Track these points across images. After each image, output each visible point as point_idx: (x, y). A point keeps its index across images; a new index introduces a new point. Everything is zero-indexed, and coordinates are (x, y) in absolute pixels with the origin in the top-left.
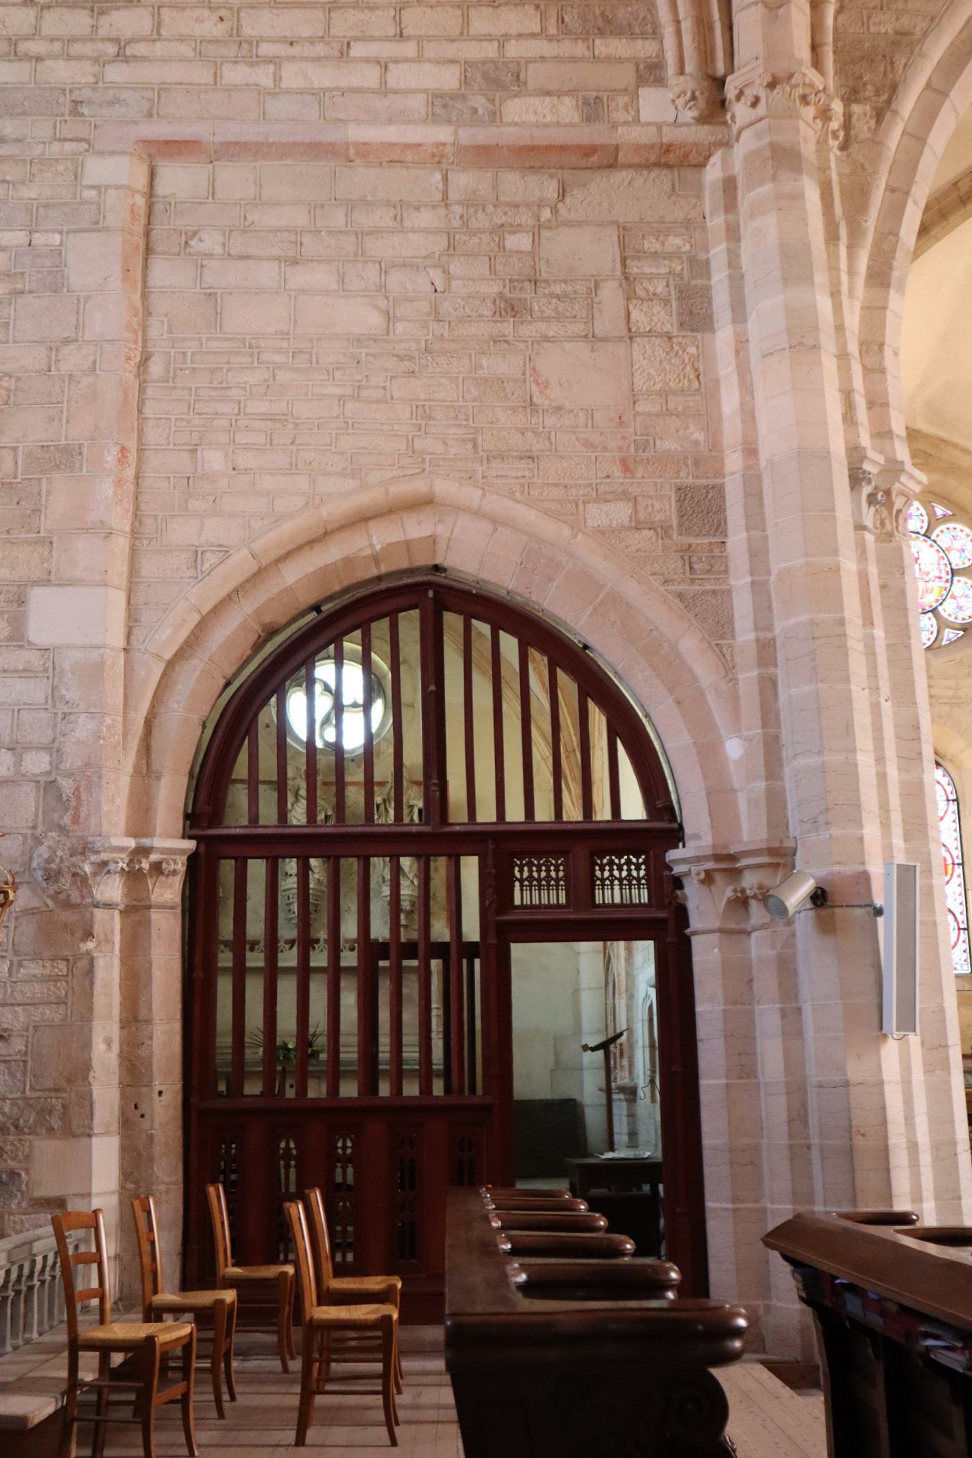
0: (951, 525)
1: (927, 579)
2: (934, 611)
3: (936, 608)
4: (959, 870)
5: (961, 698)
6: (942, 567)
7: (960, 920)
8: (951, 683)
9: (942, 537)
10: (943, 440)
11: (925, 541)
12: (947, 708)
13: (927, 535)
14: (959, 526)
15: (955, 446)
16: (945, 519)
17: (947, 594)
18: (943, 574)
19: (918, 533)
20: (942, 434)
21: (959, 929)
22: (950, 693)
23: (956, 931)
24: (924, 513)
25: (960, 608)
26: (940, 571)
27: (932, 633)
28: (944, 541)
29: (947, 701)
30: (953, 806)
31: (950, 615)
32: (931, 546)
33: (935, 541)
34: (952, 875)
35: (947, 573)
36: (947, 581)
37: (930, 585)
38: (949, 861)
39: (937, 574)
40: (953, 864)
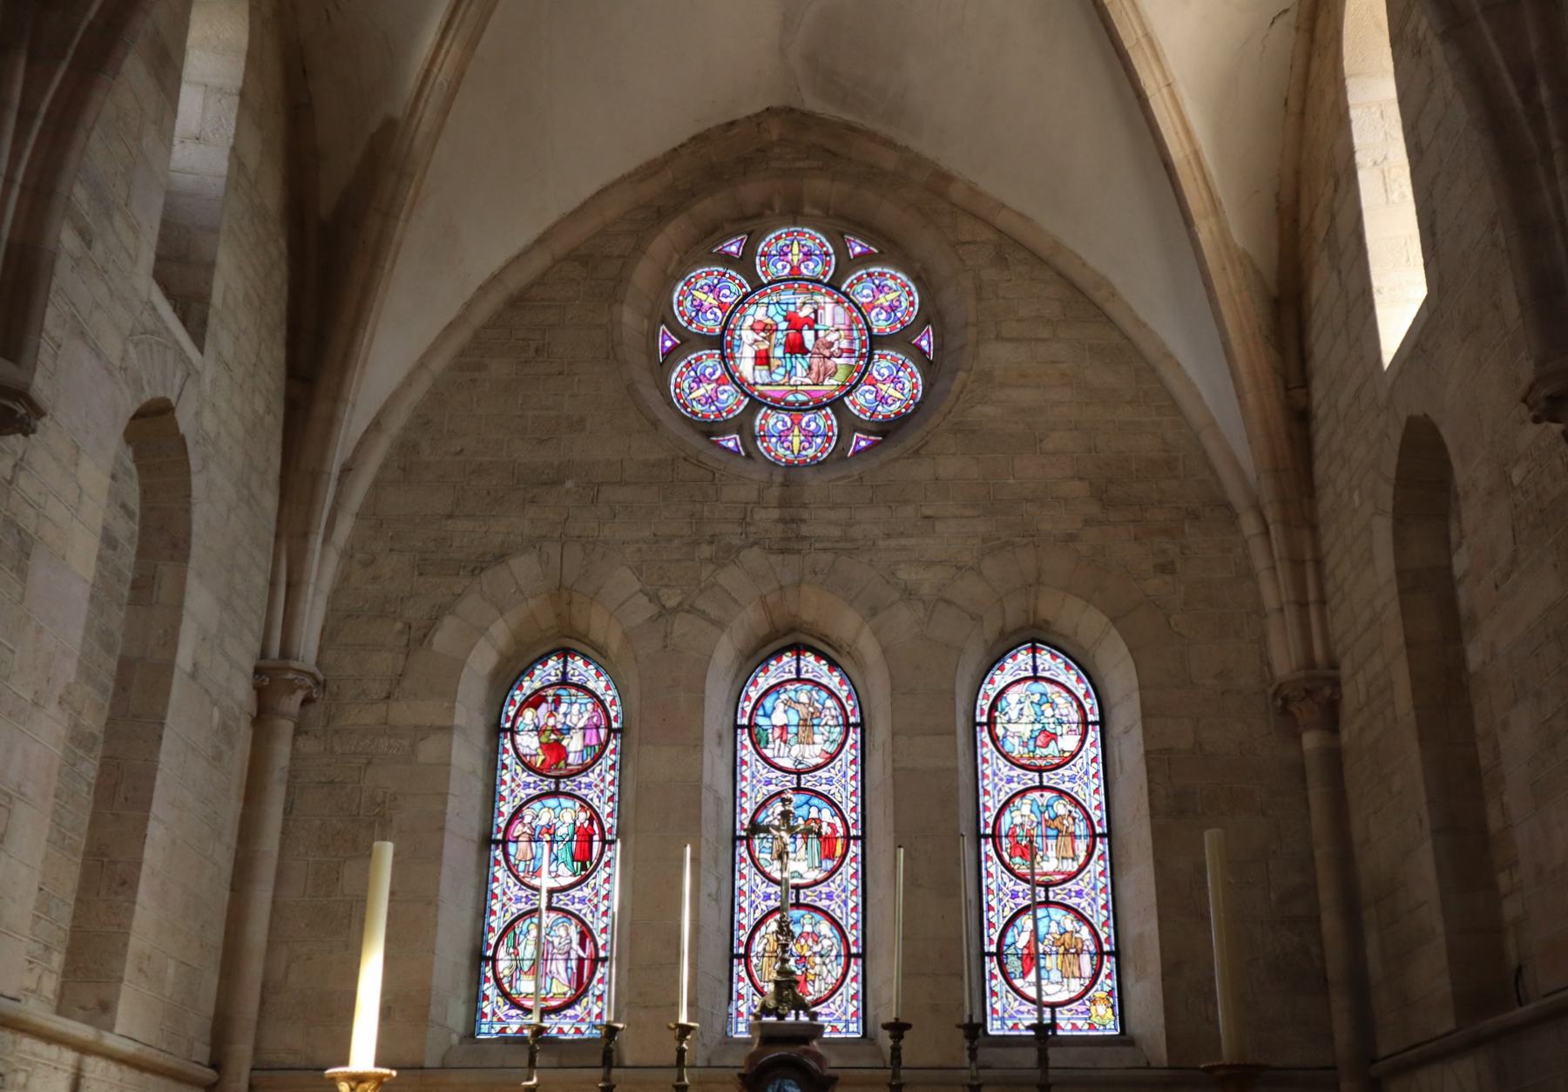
0: (875, 270)
1: (827, 353)
2: (837, 405)
3: (841, 398)
4: (855, 849)
5: (854, 540)
6: (855, 334)
7: (851, 939)
8: (842, 514)
9: (858, 288)
10: (851, 128)
11: (831, 295)
12: (827, 558)
13: (834, 285)
14: (889, 271)
15: (872, 136)
16: (865, 259)
17: (861, 376)
18: (857, 345)
19: (819, 281)
20: (849, 117)
21: (849, 956)
22: (836, 532)
23: (842, 960)
24: (831, 251)
25: (882, 400)
26: (852, 341)
27: (829, 439)
28: (863, 294)
29: (829, 545)
30: (854, 736)
31: (861, 411)
32: (838, 302)
33: (846, 294)
34: (844, 856)
35: (863, 345)
36: (862, 356)
37: (829, 363)
38: (841, 831)
39: (844, 344)
40: (847, 837)
